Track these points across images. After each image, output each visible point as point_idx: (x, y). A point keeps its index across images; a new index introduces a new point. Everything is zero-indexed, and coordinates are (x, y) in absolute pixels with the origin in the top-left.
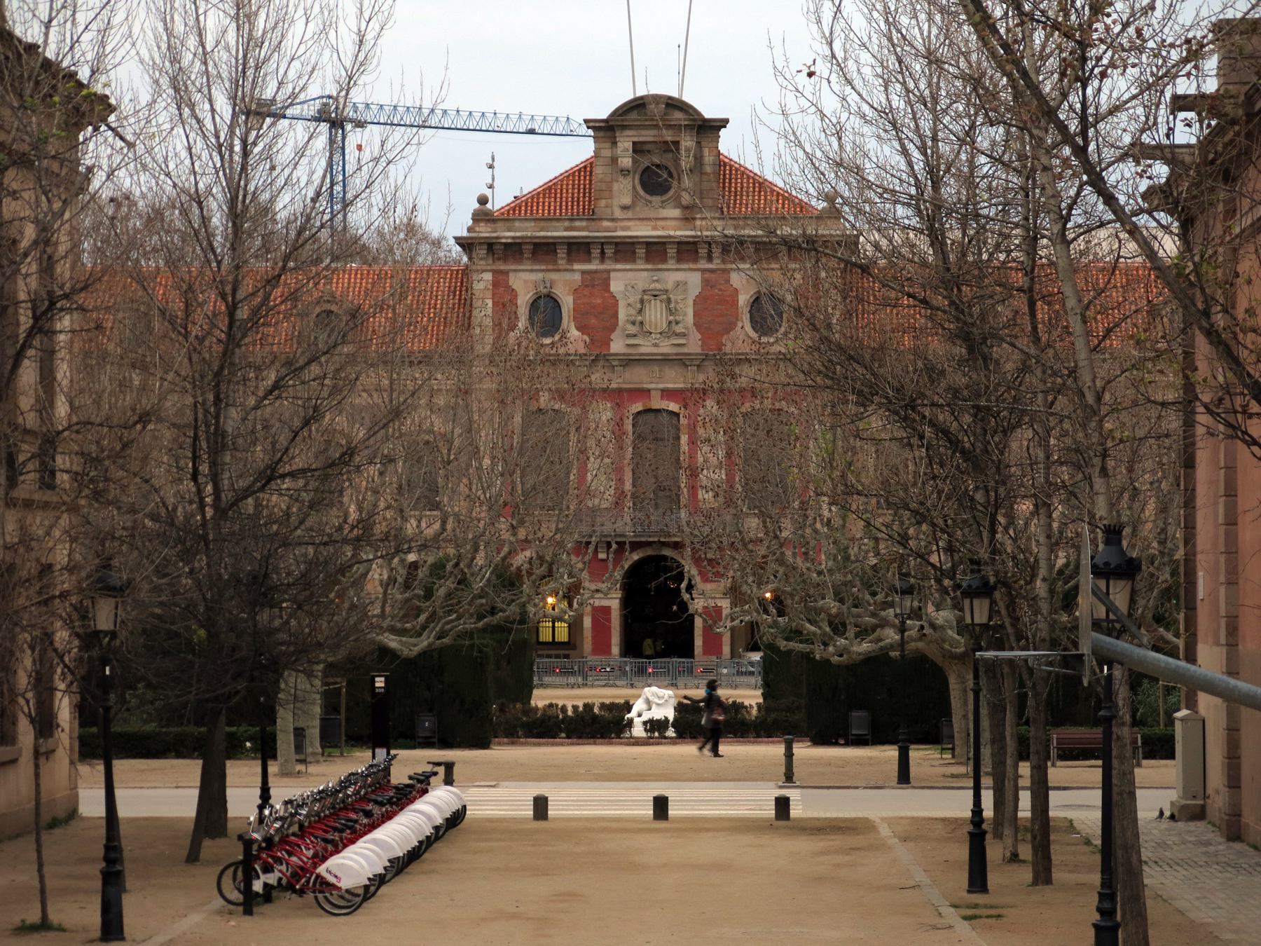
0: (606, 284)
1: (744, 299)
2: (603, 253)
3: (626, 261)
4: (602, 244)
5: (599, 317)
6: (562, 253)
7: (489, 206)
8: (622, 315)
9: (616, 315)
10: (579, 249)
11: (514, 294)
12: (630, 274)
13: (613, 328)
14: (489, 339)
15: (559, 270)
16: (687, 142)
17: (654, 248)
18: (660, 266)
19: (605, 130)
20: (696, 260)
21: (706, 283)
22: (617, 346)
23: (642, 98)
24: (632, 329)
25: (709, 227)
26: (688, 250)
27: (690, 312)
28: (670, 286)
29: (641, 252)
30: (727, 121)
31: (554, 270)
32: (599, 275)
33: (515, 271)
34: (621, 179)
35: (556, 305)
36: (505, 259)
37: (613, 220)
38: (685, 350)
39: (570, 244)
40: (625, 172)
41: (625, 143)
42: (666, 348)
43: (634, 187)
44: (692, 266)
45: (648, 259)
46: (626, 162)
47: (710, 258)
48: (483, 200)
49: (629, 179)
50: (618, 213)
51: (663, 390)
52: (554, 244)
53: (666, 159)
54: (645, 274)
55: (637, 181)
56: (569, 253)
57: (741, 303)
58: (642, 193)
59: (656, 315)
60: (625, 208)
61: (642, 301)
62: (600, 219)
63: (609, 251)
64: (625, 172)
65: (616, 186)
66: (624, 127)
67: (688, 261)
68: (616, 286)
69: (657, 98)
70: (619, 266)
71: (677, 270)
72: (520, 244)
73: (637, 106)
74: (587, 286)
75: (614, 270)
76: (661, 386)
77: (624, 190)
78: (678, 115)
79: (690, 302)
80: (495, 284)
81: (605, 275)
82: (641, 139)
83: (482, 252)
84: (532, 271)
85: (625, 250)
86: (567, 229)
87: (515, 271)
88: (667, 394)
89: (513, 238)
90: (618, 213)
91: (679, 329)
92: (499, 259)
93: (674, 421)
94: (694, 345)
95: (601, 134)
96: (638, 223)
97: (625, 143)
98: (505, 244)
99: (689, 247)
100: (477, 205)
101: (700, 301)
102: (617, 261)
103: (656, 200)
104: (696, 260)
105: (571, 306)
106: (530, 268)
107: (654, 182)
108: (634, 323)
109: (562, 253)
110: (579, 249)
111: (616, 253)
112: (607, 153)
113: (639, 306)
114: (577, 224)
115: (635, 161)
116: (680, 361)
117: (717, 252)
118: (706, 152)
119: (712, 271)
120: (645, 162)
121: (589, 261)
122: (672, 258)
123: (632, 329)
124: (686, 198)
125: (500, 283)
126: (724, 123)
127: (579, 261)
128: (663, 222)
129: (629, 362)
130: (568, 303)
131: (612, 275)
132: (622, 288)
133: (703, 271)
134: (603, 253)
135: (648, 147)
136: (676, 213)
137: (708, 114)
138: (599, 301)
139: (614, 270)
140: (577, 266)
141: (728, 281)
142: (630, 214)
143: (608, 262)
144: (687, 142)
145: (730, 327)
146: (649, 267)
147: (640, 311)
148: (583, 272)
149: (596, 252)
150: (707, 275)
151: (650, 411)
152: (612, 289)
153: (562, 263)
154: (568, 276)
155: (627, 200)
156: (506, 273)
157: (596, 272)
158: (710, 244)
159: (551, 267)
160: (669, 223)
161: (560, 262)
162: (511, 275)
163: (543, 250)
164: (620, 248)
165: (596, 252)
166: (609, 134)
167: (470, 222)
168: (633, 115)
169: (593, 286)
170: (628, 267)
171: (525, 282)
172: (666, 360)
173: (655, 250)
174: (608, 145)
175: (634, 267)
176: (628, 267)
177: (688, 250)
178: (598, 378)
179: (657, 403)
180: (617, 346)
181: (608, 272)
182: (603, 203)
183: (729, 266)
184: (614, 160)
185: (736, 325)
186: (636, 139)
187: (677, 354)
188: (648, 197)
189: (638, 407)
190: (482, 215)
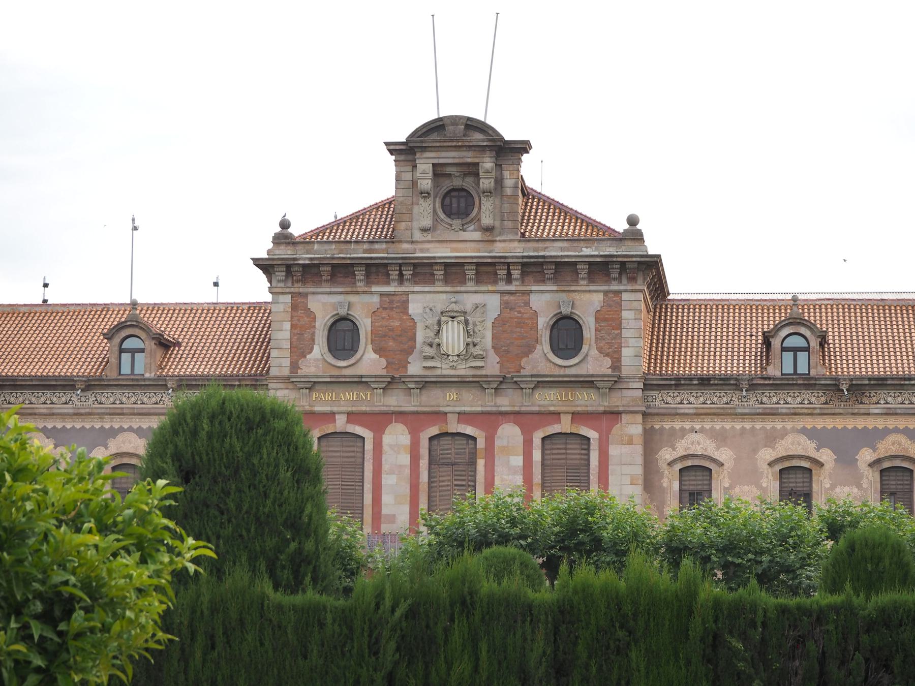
0: (405, 305)
1: (543, 322)
2: (401, 275)
3: (425, 283)
4: (400, 265)
5: (397, 340)
6: (360, 274)
7: (290, 230)
8: (421, 336)
9: (413, 338)
10: (376, 270)
12: (428, 296)
13: (410, 350)
14: (286, 362)
15: (358, 293)
16: (487, 164)
17: (454, 269)
18: (458, 289)
19: (404, 152)
21: (505, 305)
22: (415, 368)
24: (430, 351)
25: (509, 248)
26: (487, 271)
27: (489, 335)
28: (469, 307)
29: (439, 274)
30: (527, 143)
31: (352, 293)
32: (397, 298)
33: (314, 293)
34: (421, 201)
35: (355, 329)
36: (303, 281)
37: (412, 242)
38: (483, 372)
39: (368, 266)
40: (425, 194)
41: (425, 166)
42: (463, 370)
44: (490, 288)
45: (447, 281)
46: (426, 184)
47: (509, 279)
48: (285, 225)
49: (430, 201)
50: (418, 236)
51: (459, 413)
52: (352, 265)
53: (468, 183)
54: (444, 296)
55: (438, 205)
56: (368, 275)
57: (540, 326)
58: (443, 216)
59: (453, 337)
60: (424, 230)
61: (439, 323)
62: (400, 242)
63: (407, 273)
64: (425, 194)
65: (416, 209)
66: (424, 149)
67: (487, 283)
68: (415, 307)
69: (455, 120)
71: (476, 292)
72: (318, 266)
73: (437, 127)
74: (385, 309)
75: (413, 292)
76: (458, 409)
77: (424, 212)
78: (478, 136)
79: (489, 324)
80: (294, 307)
81: (404, 298)
82: (442, 161)
83: (281, 275)
84: (330, 293)
85: (422, 271)
86: (365, 251)
87: (314, 293)
88: (464, 417)
89: (311, 259)
90: (418, 236)
91: (476, 351)
92: (298, 281)
93: (471, 442)
94: (492, 366)
95: (402, 157)
96: (437, 245)
97: (425, 166)
98: (304, 266)
99: (489, 269)
100: (279, 229)
101: (499, 323)
102: (416, 283)
103: (457, 223)
104: (495, 282)
105: (369, 329)
106: (328, 290)
107: (457, 203)
108: (431, 345)
109: (360, 274)
110: (376, 270)
111: (414, 275)
112: (408, 176)
113: (436, 327)
114: (377, 246)
115: (436, 185)
116: (477, 383)
117: (516, 274)
118: (506, 174)
119: (511, 293)
120: (447, 185)
121: (388, 283)
122: (471, 279)
123: (430, 351)
124: (486, 221)
125: (298, 306)
126: (523, 147)
127: (378, 283)
128: (462, 244)
129: (424, 384)
130: (365, 325)
131: (411, 297)
132: (420, 311)
133: (502, 293)
134: (401, 275)
135: (449, 170)
136: (477, 235)
138: (397, 324)
139: (413, 292)
140: (375, 289)
141: (527, 303)
142: (429, 237)
143: (406, 283)
144: (487, 164)
145: (529, 350)
146: (448, 289)
147: (438, 333)
148: (382, 295)
149: (394, 274)
150: (506, 298)
151: (446, 434)
152: (410, 311)
154: (366, 298)
155: (427, 222)
156: (305, 295)
157: (395, 294)
158: (508, 264)
159: (349, 289)
160: (468, 245)
161: (359, 284)
162: (310, 297)
163: (341, 272)
164: (419, 269)
166: (410, 157)
167: (271, 246)
168: (434, 136)
169: (392, 309)
170: (427, 289)
171: (324, 304)
172: (461, 383)
173: (454, 271)
174: (410, 168)
175: (432, 289)
176: (427, 289)
177: (487, 271)
178: (395, 401)
179: (454, 426)
180: (415, 368)
181: (407, 294)
182: (402, 226)
183: (528, 288)
184: (414, 183)
185: (535, 348)
186: (436, 161)
187: (474, 376)
188: (448, 220)
189: (434, 431)
190: (283, 238)
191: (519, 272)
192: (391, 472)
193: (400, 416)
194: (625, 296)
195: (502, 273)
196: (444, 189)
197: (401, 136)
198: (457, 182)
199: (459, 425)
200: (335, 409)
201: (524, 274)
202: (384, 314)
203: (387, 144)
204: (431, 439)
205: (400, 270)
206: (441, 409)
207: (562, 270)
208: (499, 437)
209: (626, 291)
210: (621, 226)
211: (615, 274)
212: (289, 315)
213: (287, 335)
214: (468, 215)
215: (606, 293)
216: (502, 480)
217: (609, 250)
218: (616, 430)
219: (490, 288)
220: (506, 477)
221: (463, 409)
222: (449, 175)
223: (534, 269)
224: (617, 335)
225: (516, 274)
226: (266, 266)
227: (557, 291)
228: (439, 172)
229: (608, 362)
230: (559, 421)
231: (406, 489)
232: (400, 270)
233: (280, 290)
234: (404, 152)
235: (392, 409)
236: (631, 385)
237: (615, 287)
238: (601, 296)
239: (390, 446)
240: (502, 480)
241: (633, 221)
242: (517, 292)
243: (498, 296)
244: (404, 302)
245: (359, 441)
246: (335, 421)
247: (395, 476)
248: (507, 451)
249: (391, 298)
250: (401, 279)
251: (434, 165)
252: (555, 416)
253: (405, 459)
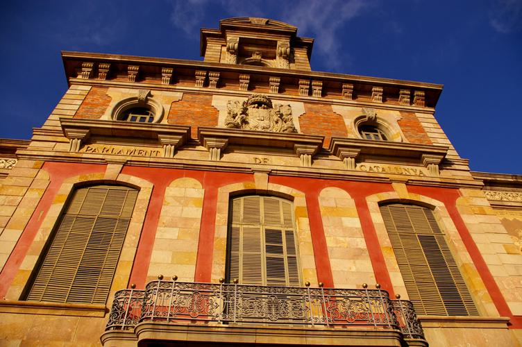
0: (208, 103)
1: (349, 122)
4: (208, 70)
11: (109, 99)
15: (161, 89)
32: (201, 97)
51: (270, 173)
76: (268, 168)
105: (167, 111)
139: (218, 94)
141: (331, 111)
148: (185, 92)
149: (200, 80)
150: (310, 105)
153: (165, 84)
157: (199, 93)
158: (311, 79)
189: (238, 187)
191: (321, 88)
192: (172, 225)
193: (192, 170)
194: (418, 115)
199: (270, 184)
200: (108, 158)
202: (186, 104)
204: (233, 196)
205: (207, 76)
206: (247, 166)
208: (324, 198)
209: (419, 111)
212: (83, 97)
213: (77, 107)
215: (401, 111)
216: (337, 242)
218: (459, 201)
219: (294, 97)
220: (342, 239)
221: (275, 168)
224: (424, 136)
225: (317, 90)
227: (357, 105)
228: (243, 42)
230: (392, 190)
231: (192, 245)
232: (207, 76)
233: (83, 81)
235: (184, 162)
236: (457, 167)
238: (398, 113)
239: (175, 198)
240: (337, 242)
242: (318, 102)
243: (301, 105)
244: (207, 100)
245: (133, 193)
246: (105, 169)
247: (176, 230)
248: (336, 211)
249: (194, 96)
251: (240, 38)
252: (386, 184)
253: (196, 213)
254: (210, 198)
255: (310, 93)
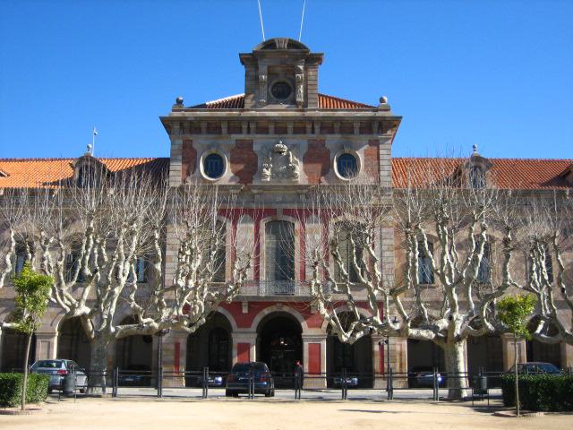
2: (249, 128)
14: (180, 179)
19: (250, 60)
20: (305, 132)
23: (273, 40)
43: (268, 93)
55: (270, 89)
58: (272, 96)
63: (253, 126)
70: (258, 136)
80: (184, 146)
83: (176, 127)
110: (235, 126)
112: (252, 74)
121: (241, 133)
134: (249, 128)
135: (278, 70)
136: (294, 107)
137: (313, 50)
140: (233, 136)
163: (213, 127)
165: (245, 127)
173: (280, 127)
174: (253, 69)
175: (267, 136)
177: (301, 126)
184: (257, 78)
195: (309, 127)
196: (274, 82)
197: (249, 49)
198: (282, 79)
201: (321, 128)
203: (240, 55)
207: (345, 127)
210: (376, 103)
211: (375, 130)
214: (289, 87)
217: (370, 114)
222: (277, 75)
223: (328, 126)
226: (167, 123)
229: (372, 180)
234: (250, 60)
237: (376, 136)
241: (382, 100)
250: (249, 132)
254: (257, 228)
255: (313, 132)
